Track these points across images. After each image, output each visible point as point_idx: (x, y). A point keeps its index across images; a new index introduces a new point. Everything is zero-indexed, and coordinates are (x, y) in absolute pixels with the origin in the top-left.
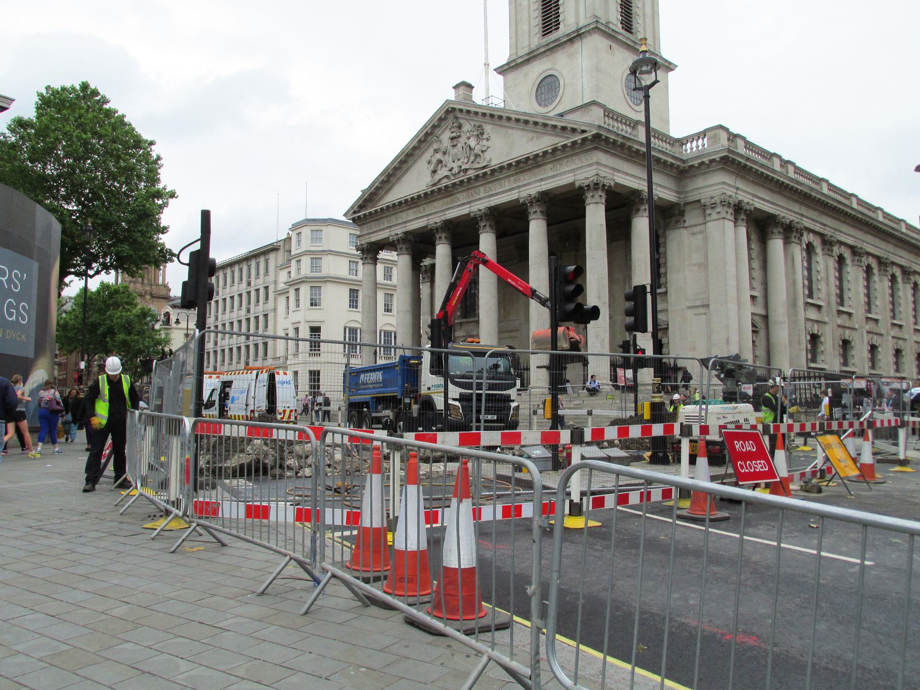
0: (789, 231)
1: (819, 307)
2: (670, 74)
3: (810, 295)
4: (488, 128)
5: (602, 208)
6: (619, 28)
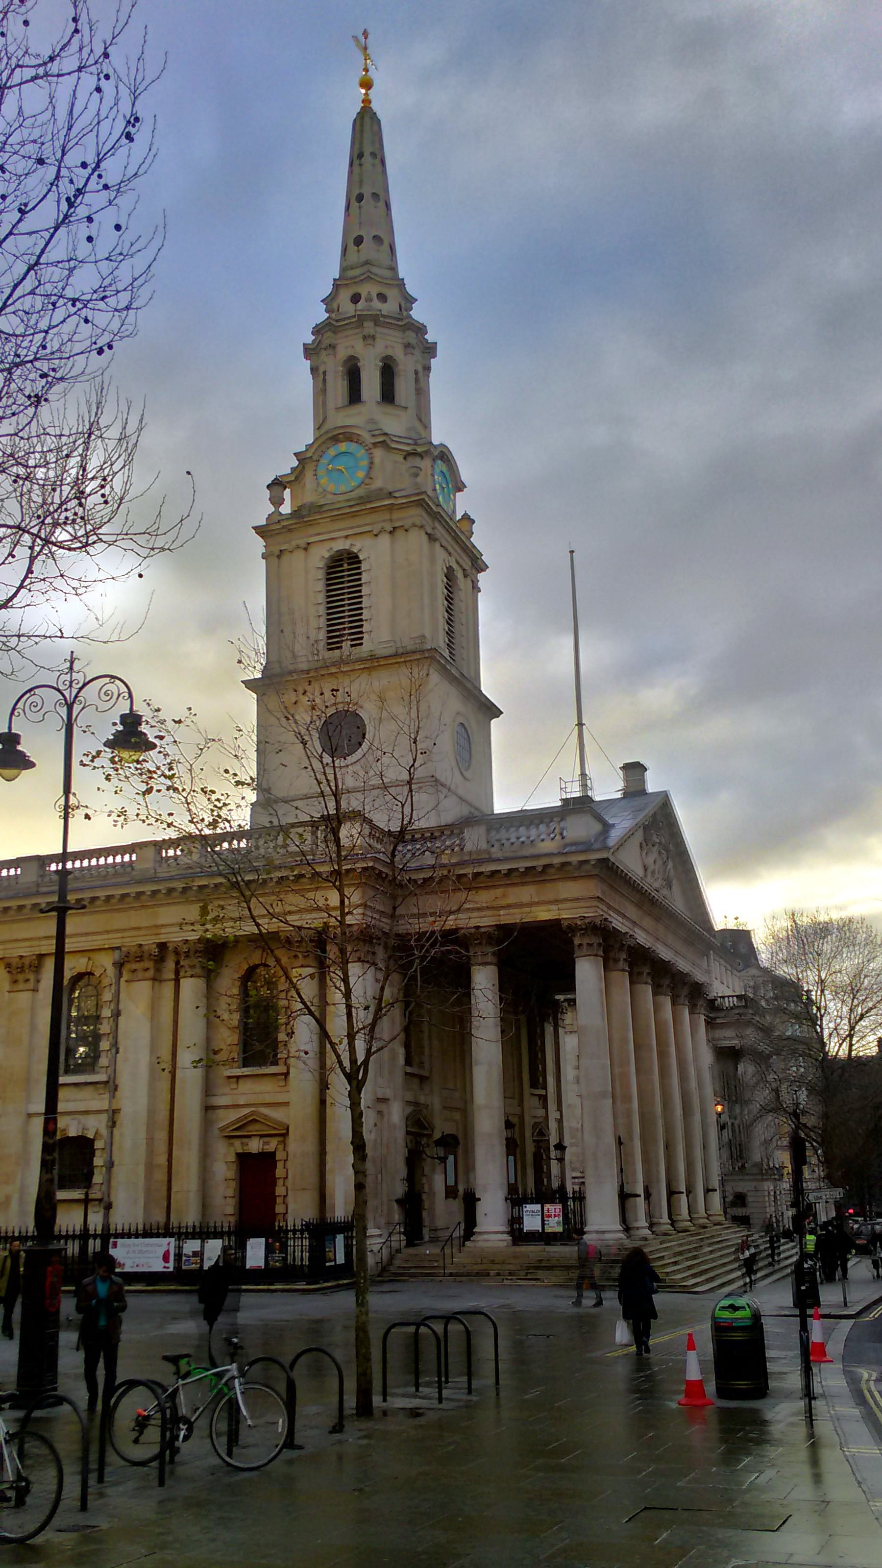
2: (494, 722)
6: (446, 654)
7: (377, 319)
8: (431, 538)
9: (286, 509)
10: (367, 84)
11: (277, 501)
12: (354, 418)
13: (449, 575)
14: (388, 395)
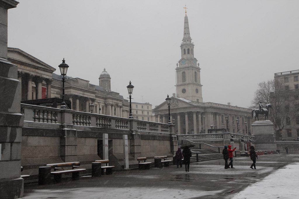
0: (219, 114)
1: (224, 124)
3: (223, 123)
4: (179, 101)
5: (195, 115)
7: (187, 44)
8: (192, 70)
9: (178, 66)
10: (186, 12)
11: (177, 66)
12: (185, 57)
13: (196, 72)
14: (188, 53)
